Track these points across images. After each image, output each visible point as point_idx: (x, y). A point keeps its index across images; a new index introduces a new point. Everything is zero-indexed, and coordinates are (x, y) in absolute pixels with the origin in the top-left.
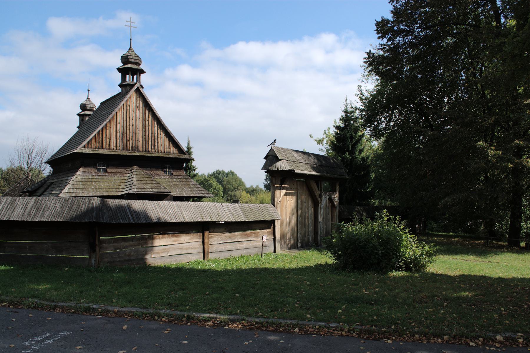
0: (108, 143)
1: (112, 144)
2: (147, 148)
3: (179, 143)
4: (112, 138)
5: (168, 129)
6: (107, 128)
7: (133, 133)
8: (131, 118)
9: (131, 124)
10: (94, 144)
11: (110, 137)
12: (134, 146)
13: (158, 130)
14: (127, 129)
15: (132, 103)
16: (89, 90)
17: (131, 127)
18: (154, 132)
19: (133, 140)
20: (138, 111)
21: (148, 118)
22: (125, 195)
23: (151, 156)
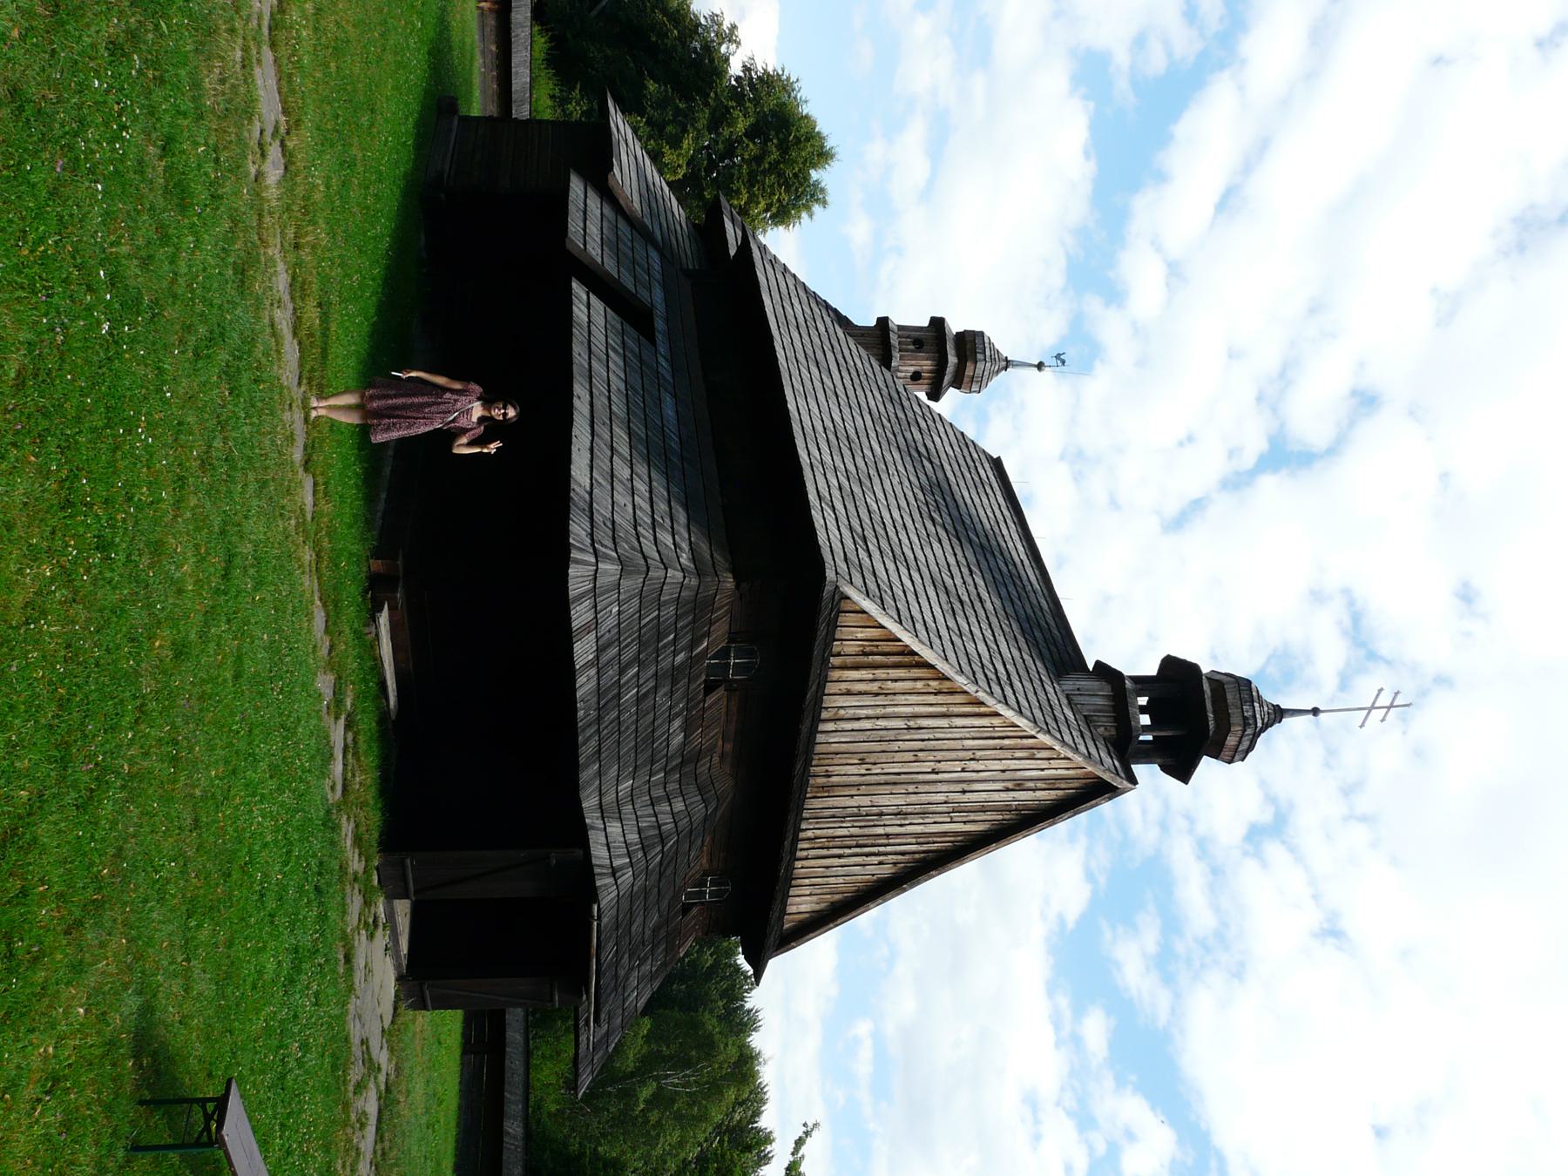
1: (852, 701)
4: (880, 700)
5: (905, 890)
6: (934, 684)
7: (899, 774)
8: (973, 765)
9: (942, 766)
10: (860, 636)
11: (886, 694)
12: (834, 779)
13: (903, 853)
14: (920, 754)
15: (1044, 764)
16: (1040, 366)
17: (927, 767)
18: (891, 841)
21: (964, 819)
22: (580, 853)
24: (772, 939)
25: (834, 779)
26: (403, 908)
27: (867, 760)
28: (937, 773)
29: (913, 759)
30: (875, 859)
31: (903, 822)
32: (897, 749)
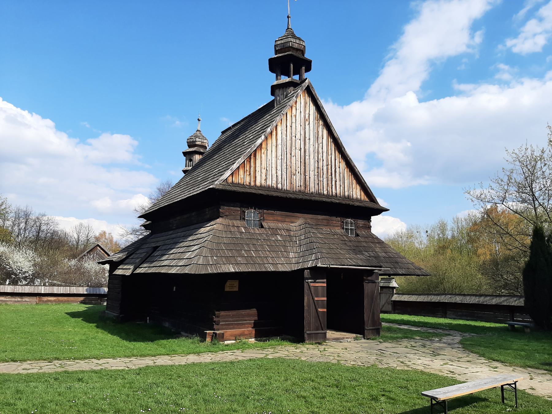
0: (264, 177)
2: (321, 190)
3: (366, 183)
5: (350, 159)
7: (301, 162)
8: (298, 136)
10: (242, 176)
15: (298, 111)
18: (330, 164)
19: (301, 174)
20: (307, 127)
23: (332, 202)
24: (371, 205)
25: (302, 184)
26: (330, 334)
27: (294, 173)
28: (301, 149)
29: (294, 157)
30: (338, 170)
31: (322, 160)
32: (290, 163)
